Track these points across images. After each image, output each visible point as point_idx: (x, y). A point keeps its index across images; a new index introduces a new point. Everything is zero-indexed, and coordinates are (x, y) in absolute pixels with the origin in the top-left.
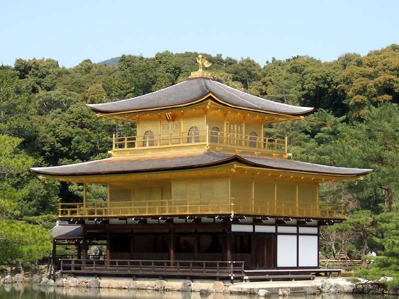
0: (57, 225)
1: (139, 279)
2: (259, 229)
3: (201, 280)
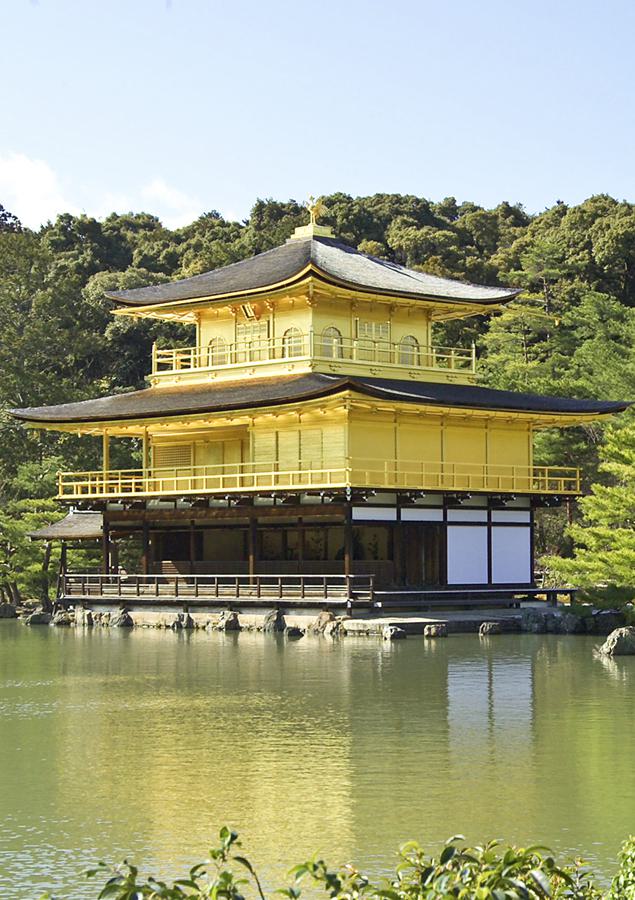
0: (71, 513)
1: (196, 609)
2: (408, 515)
3: (299, 610)
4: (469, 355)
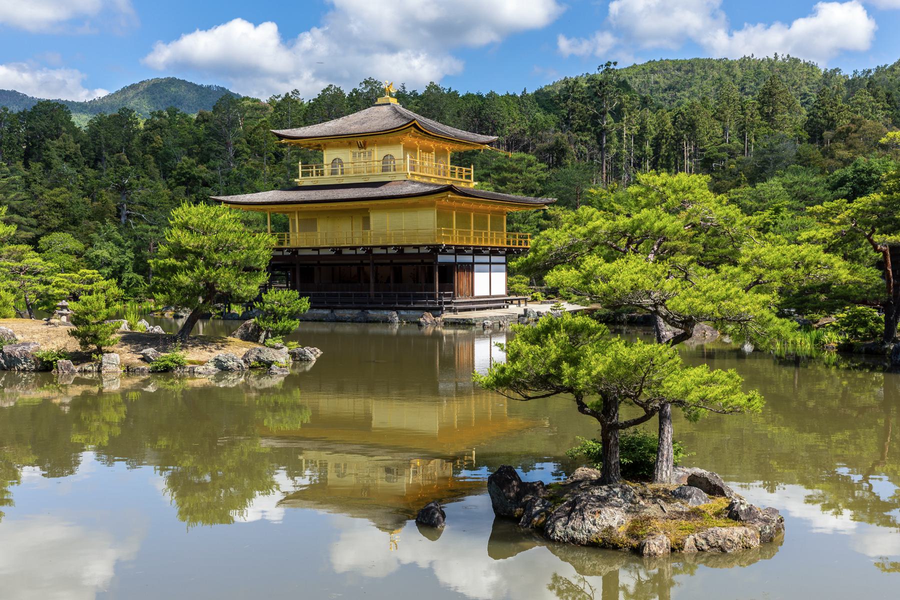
2: (461, 259)
4: (470, 171)
